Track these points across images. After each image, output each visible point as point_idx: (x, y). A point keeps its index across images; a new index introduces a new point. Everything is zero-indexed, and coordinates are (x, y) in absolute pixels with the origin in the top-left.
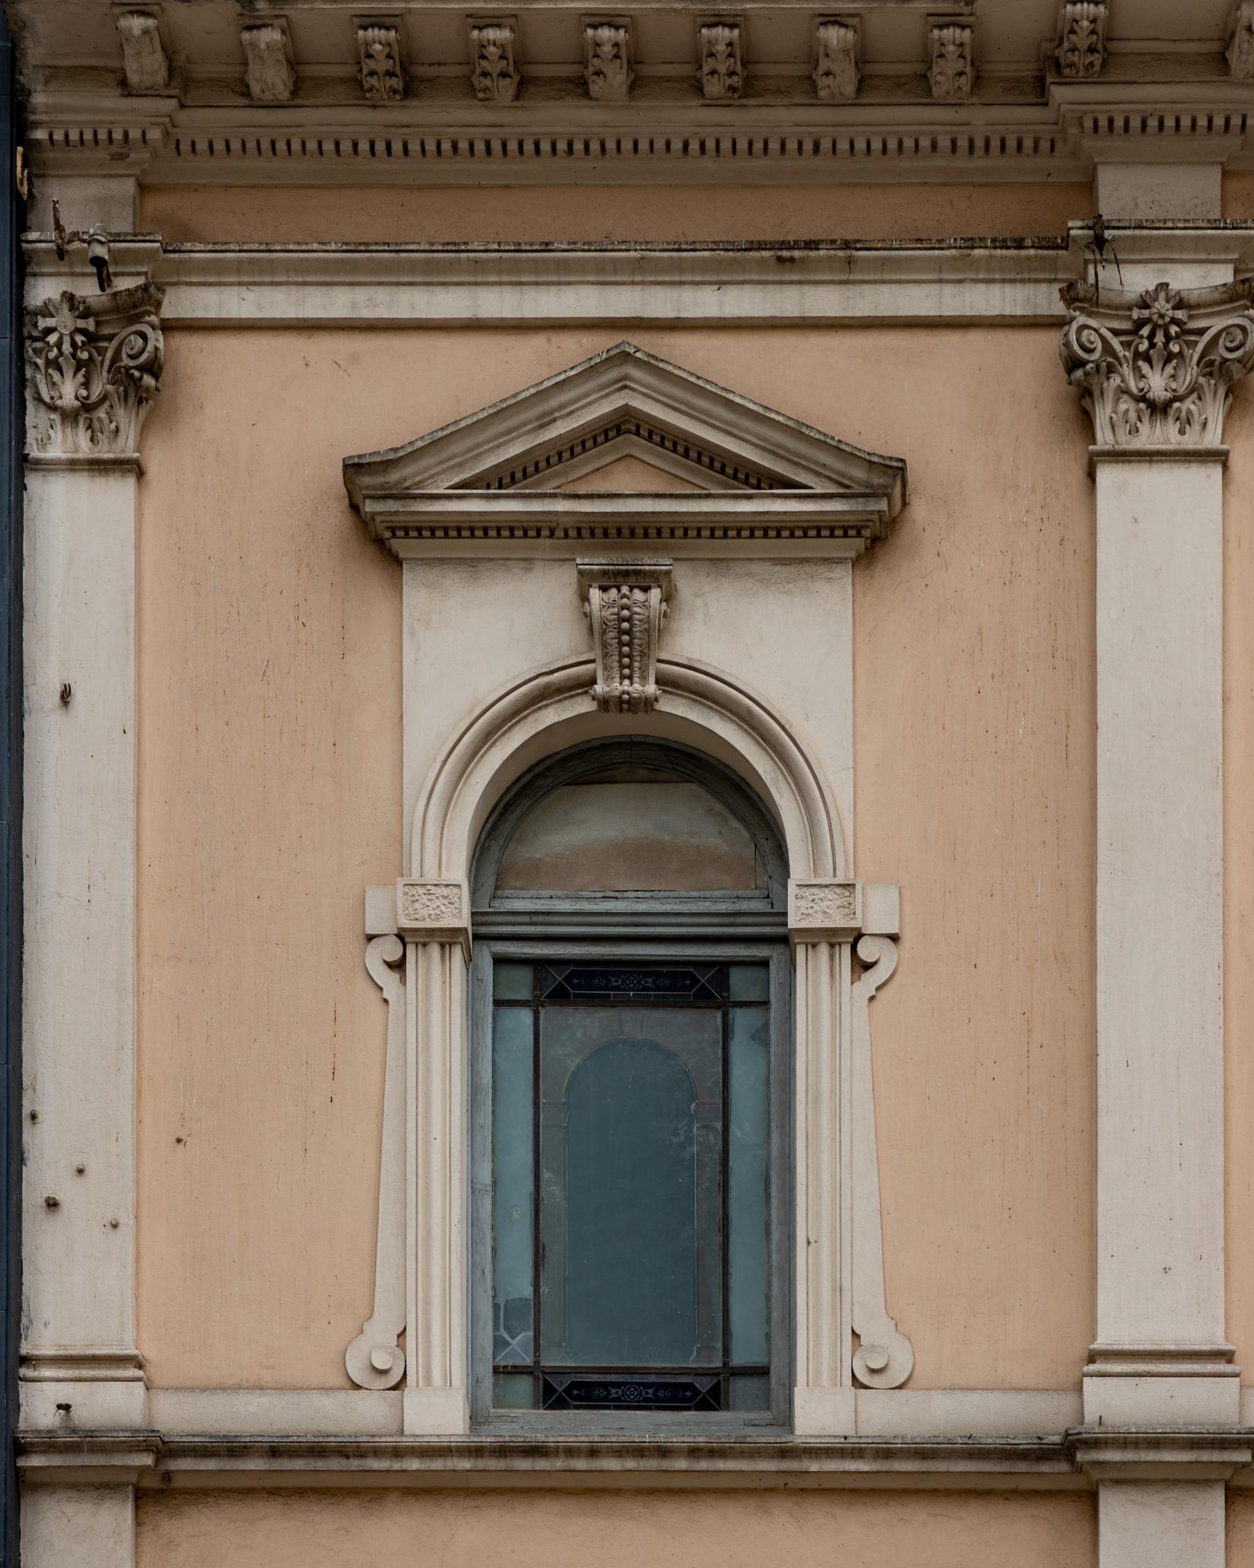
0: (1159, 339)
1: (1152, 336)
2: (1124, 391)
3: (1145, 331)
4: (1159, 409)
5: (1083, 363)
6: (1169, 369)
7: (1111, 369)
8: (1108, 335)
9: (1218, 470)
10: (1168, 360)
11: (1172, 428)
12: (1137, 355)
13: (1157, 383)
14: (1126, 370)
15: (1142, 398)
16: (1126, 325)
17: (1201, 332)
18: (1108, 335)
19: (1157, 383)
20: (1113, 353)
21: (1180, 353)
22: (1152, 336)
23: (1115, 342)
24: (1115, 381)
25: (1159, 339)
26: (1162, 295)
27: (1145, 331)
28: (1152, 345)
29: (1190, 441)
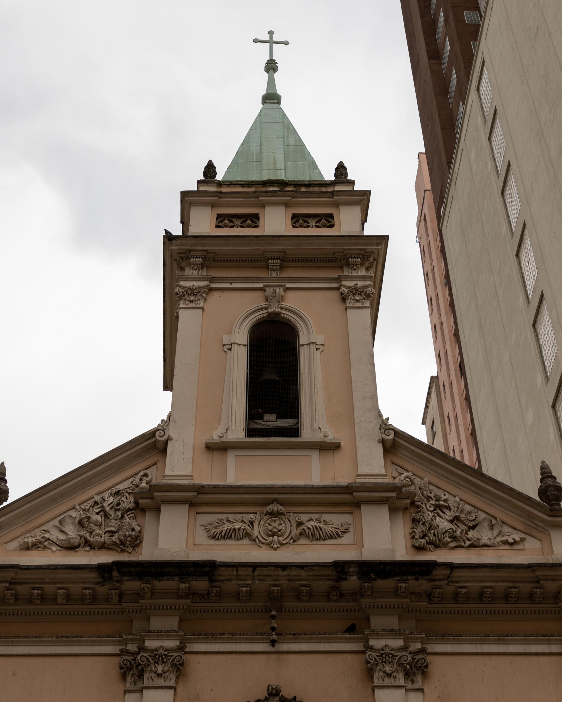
0: (160, 659)
1: (159, 658)
2: (151, 671)
3: (157, 657)
4: (159, 675)
5: (140, 665)
6: (163, 666)
7: (149, 665)
8: (148, 657)
9: (172, 691)
10: (162, 664)
11: (162, 680)
12: (155, 662)
13: (160, 669)
14: (152, 666)
15: (155, 672)
16: (153, 655)
17: (172, 656)
18: (148, 657)
19: (160, 669)
20: (149, 661)
21: (167, 661)
22: (159, 658)
23: (150, 659)
24: (149, 668)
25: (160, 659)
26: (161, 649)
27: (157, 657)
28: (159, 660)
29: (169, 683)
